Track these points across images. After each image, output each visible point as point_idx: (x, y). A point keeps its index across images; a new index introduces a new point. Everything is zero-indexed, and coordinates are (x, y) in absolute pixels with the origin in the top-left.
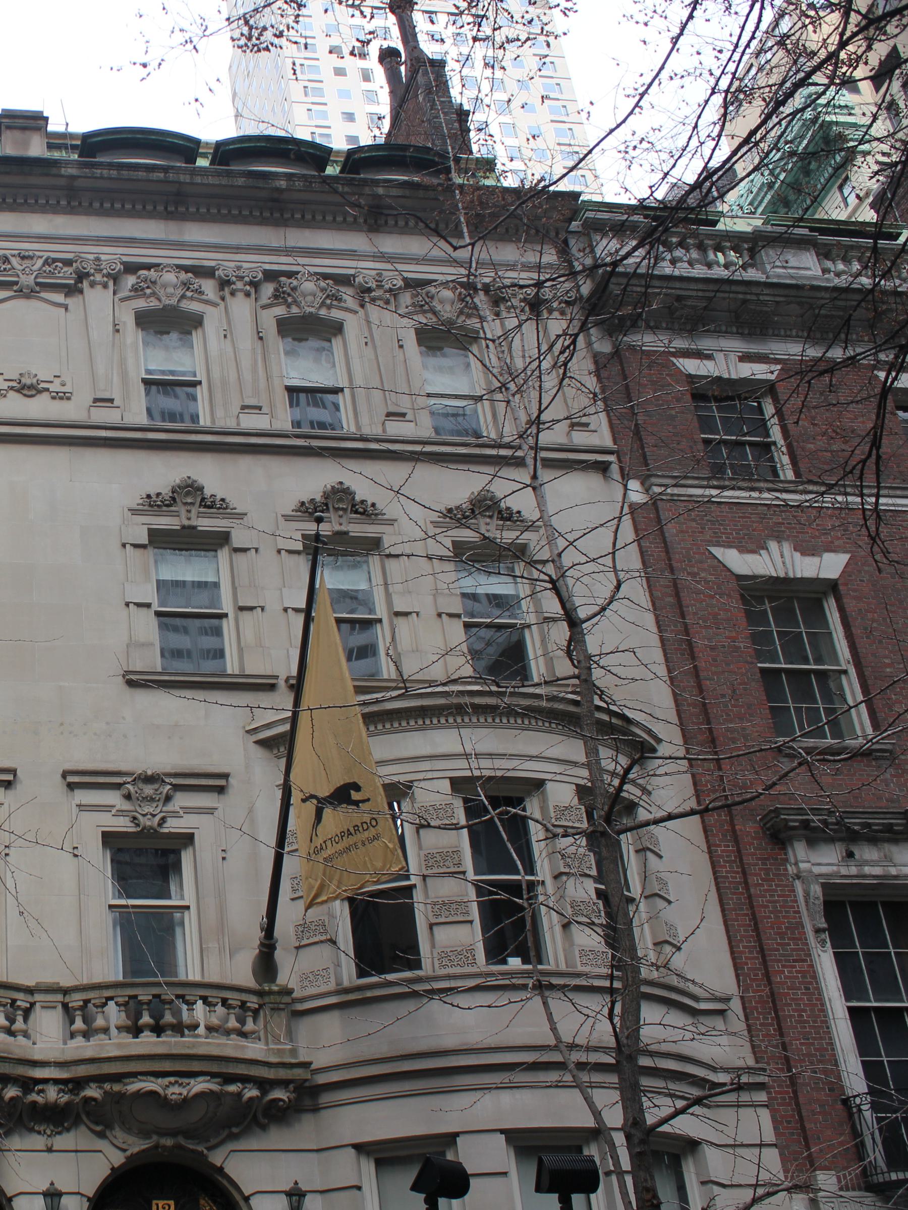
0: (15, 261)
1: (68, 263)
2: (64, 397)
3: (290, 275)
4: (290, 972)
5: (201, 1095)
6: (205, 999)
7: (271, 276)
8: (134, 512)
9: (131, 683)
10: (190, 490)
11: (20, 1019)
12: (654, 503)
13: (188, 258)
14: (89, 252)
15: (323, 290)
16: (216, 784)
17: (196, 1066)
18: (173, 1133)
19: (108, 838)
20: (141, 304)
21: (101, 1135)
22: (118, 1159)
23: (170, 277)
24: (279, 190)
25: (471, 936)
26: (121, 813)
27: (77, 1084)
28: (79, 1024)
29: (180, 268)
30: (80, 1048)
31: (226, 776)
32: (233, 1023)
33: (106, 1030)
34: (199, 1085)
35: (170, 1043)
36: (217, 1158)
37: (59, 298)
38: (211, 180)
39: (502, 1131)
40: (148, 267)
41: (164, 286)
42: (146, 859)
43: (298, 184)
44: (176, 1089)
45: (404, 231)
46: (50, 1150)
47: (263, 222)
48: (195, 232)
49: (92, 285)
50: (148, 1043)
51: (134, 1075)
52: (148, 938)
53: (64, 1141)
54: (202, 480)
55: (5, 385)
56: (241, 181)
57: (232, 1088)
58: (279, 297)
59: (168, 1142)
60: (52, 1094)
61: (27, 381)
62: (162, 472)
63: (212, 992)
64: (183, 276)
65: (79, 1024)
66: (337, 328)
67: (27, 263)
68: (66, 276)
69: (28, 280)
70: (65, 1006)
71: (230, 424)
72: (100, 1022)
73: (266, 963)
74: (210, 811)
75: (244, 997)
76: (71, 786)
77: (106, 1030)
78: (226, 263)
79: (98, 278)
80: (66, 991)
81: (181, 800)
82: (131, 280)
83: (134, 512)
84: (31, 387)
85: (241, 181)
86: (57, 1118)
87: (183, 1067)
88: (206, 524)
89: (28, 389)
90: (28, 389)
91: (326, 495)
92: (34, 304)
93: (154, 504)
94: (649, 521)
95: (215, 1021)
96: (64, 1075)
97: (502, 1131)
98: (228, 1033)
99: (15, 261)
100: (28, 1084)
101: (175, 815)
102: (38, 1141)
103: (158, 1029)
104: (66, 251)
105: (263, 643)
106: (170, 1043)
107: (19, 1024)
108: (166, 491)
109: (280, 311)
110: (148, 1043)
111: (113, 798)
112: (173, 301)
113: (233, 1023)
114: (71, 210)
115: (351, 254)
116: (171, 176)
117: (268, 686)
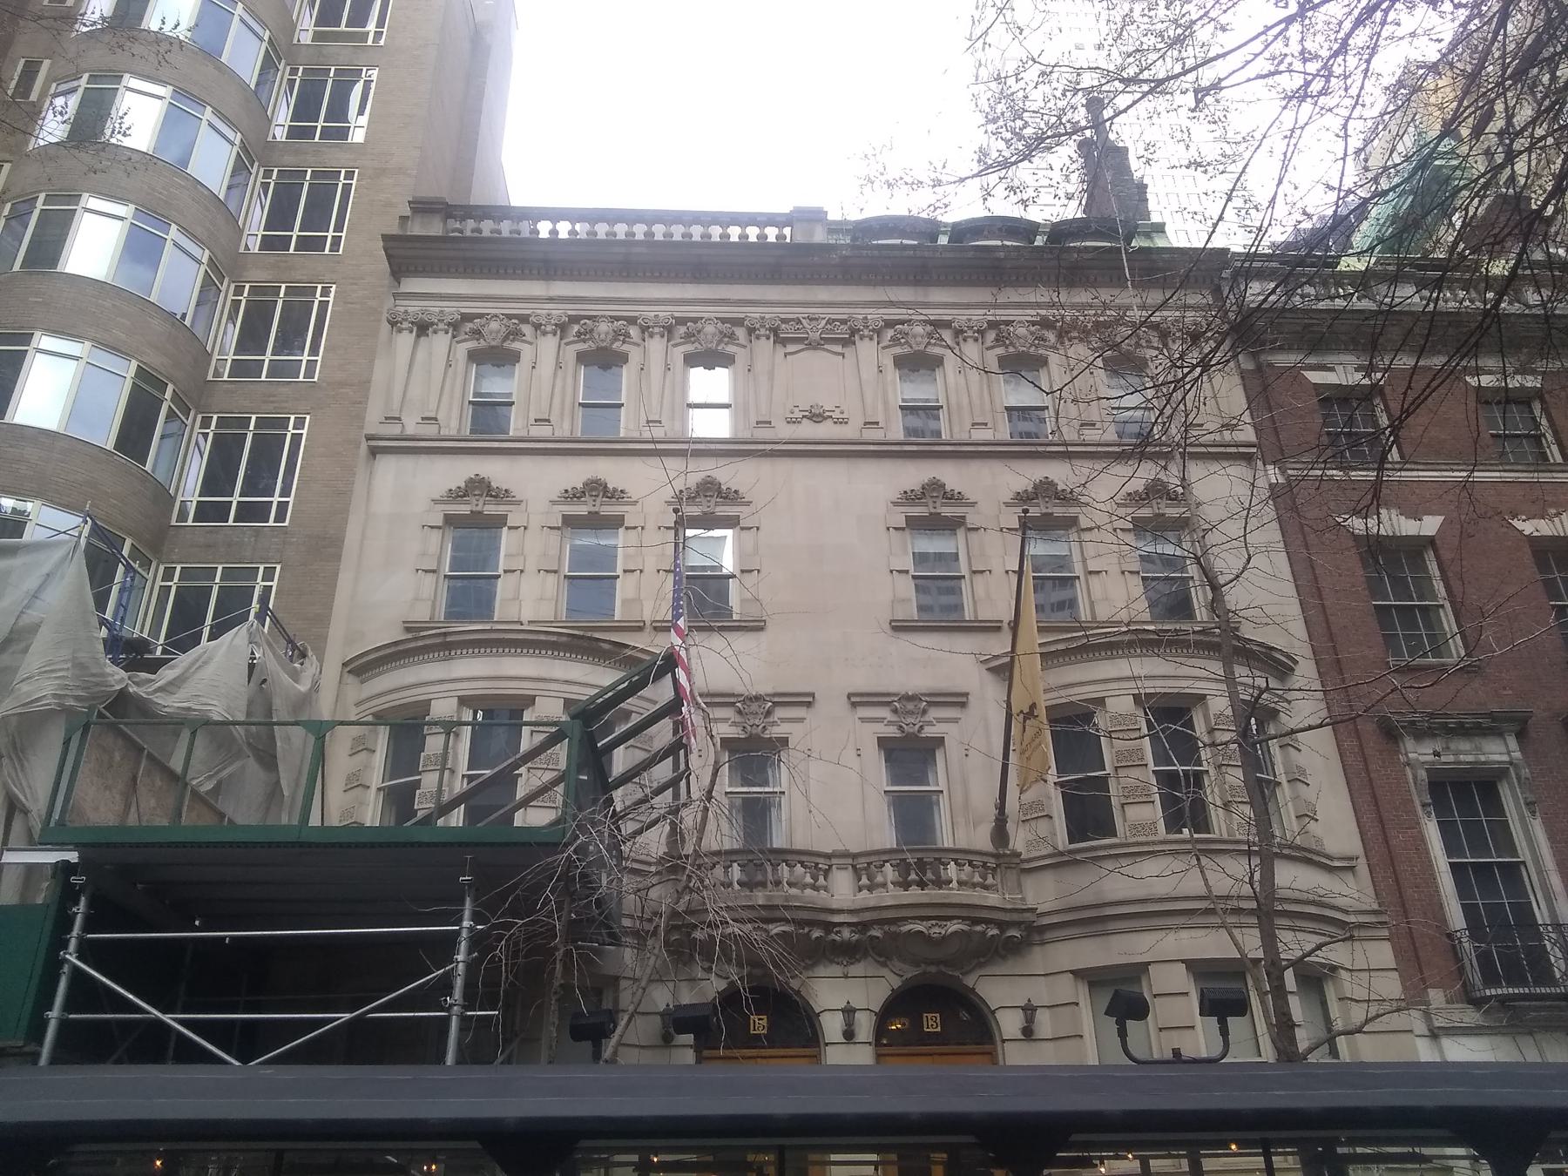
1: (844, 322)
2: (844, 422)
4: (1019, 840)
5: (956, 932)
6: (956, 861)
7: (993, 325)
8: (895, 504)
10: (934, 489)
11: (821, 879)
13: (933, 314)
14: (860, 313)
15: (1032, 333)
16: (959, 700)
17: (950, 912)
18: (938, 963)
19: (882, 742)
20: (898, 350)
21: (884, 965)
22: (897, 982)
23: (919, 329)
24: (999, 259)
25: (1153, 813)
26: (890, 723)
27: (863, 926)
28: (864, 881)
30: (867, 898)
31: (966, 695)
32: (977, 879)
33: (884, 885)
34: (954, 927)
35: (932, 894)
36: (969, 981)
37: (838, 348)
39: (1183, 961)
40: (902, 322)
41: (915, 336)
42: (909, 754)
44: (937, 930)
46: (846, 977)
50: (915, 894)
51: (905, 919)
52: (913, 814)
53: (857, 969)
54: (944, 479)
56: (970, 255)
57: (978, 928)
58: (999, 340)
59: (933, 969)
60: (846, 933)
62: (914, 475)
63: (962, 856)
64: (929, 328)
65: (864, 881)
70: (854, 867)
71: (964, 437)
72: (879, 879)
73: (1000, 833)
74: (956, 720)
75: (985, 859)
76: (854, 705)
77: (884, 885)
78: (961, 317)
79: (866, 332)
80: (855, 856)
81: (934, 713)
82: (890, 333)
83: (895, 504)
84: (819, 415)
86: (849, 953)
87: (942, 911)
88: (947, 511)
89: (816, 417)
90: (816, 417)
91: (1035, 487)
93: (909, 498)
95: (964, 877)
96: (854, 920)
97: (1183, 961)
98: (974, 885)
100: (829, 927)
101: (930, 723)
102: (836, 970)
103: (922, 884)
105: (991, 597)
106: (932, 894)
107: (821, 880)
108: (917, 488)
109: (1000, 351)
110: (915, 894)
111: (885, 713)
112: (922, 347)
113: (977, 879)
117: (999, 629)
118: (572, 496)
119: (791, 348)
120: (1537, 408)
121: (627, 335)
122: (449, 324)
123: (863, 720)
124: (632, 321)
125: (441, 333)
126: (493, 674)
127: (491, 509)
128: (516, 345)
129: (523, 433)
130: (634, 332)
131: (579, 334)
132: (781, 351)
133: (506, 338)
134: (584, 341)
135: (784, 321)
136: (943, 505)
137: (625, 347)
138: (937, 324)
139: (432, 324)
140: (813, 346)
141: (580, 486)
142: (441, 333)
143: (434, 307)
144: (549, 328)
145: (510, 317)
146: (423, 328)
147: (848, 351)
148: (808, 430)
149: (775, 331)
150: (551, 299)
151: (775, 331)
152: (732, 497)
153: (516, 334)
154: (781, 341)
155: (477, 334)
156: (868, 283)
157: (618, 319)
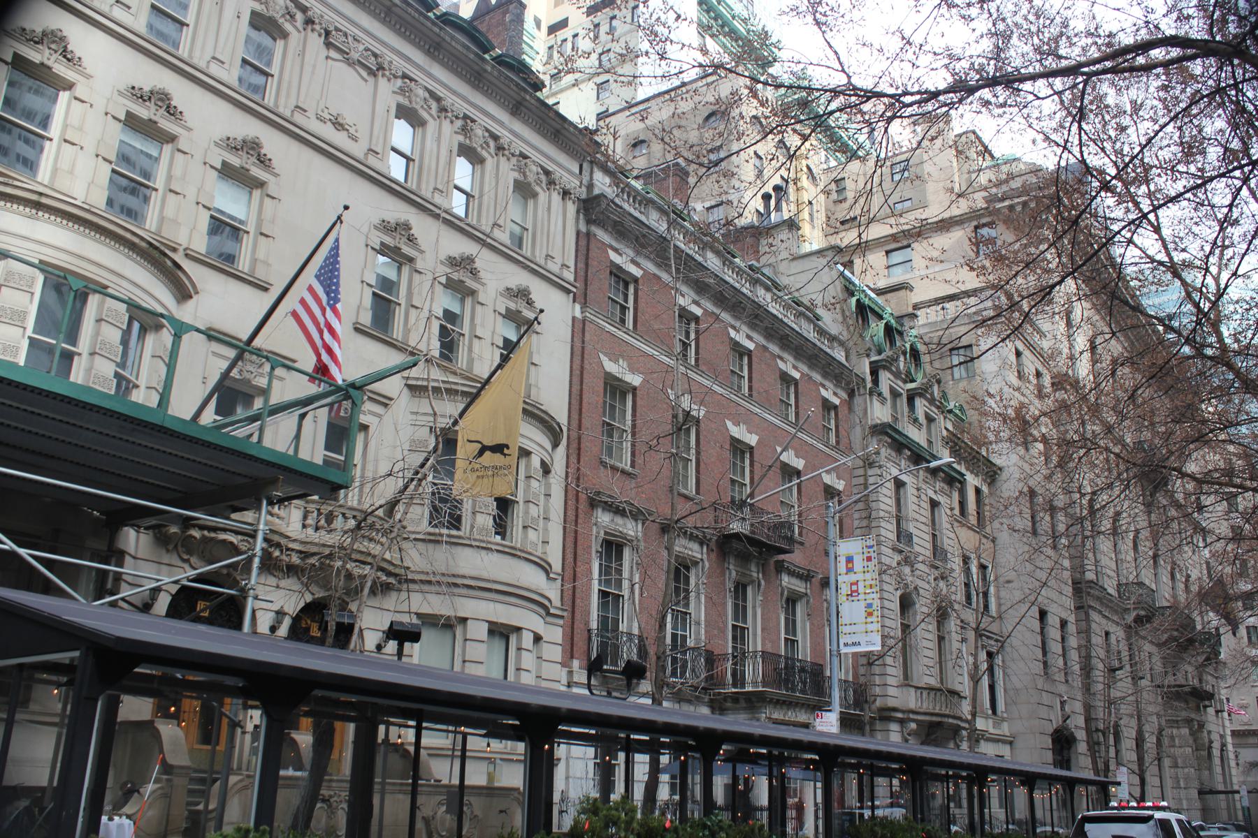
0: (350, 39)
1: (375, 55)
2: (355, 139)
3: (473, 121)
7: (466, 117)
9: (356, 329)
12: (584, 321)
14: (389, 56)
20: (401, 99)
23: (421, 92)
24: (486, 71)
29: (427, 89)
31: (391, 399)
37: (364, 74)
38: (459, 48)
40: (411, 80)
41: (417, 96)
43: (496, 73)
45: (525, 122)
47: (469, 82)
49: (383, 75)
55: (328, 117)
58: (402, 91)
62: (397, 211)
64: (427, 95)
66: (481, 161)
67: (356, 44)
74: (379, 416)
78: (449, 99)
82: (399, 82)
85: (472, 56)
88: (406, 250)
89: (338, 125)
90: (338, 125)
92: (351, 70)
93: (385, 227)
94: (579, 328)
99: (350, 39)
114: (384, 21)
115: (501, 124)
116: (442, 34)
119: (333, 54)
123: (214, 354)
132: (324, 52)
135: (337, 29)
136: (405, 243)
138: (432, 94)
140: (350, 63)
141: (147, 89)
147: (371, 80)
148: (328, 132)
149: (328, 33)
151: (328, 33)
154: (328, 45)
156: (399, 33)
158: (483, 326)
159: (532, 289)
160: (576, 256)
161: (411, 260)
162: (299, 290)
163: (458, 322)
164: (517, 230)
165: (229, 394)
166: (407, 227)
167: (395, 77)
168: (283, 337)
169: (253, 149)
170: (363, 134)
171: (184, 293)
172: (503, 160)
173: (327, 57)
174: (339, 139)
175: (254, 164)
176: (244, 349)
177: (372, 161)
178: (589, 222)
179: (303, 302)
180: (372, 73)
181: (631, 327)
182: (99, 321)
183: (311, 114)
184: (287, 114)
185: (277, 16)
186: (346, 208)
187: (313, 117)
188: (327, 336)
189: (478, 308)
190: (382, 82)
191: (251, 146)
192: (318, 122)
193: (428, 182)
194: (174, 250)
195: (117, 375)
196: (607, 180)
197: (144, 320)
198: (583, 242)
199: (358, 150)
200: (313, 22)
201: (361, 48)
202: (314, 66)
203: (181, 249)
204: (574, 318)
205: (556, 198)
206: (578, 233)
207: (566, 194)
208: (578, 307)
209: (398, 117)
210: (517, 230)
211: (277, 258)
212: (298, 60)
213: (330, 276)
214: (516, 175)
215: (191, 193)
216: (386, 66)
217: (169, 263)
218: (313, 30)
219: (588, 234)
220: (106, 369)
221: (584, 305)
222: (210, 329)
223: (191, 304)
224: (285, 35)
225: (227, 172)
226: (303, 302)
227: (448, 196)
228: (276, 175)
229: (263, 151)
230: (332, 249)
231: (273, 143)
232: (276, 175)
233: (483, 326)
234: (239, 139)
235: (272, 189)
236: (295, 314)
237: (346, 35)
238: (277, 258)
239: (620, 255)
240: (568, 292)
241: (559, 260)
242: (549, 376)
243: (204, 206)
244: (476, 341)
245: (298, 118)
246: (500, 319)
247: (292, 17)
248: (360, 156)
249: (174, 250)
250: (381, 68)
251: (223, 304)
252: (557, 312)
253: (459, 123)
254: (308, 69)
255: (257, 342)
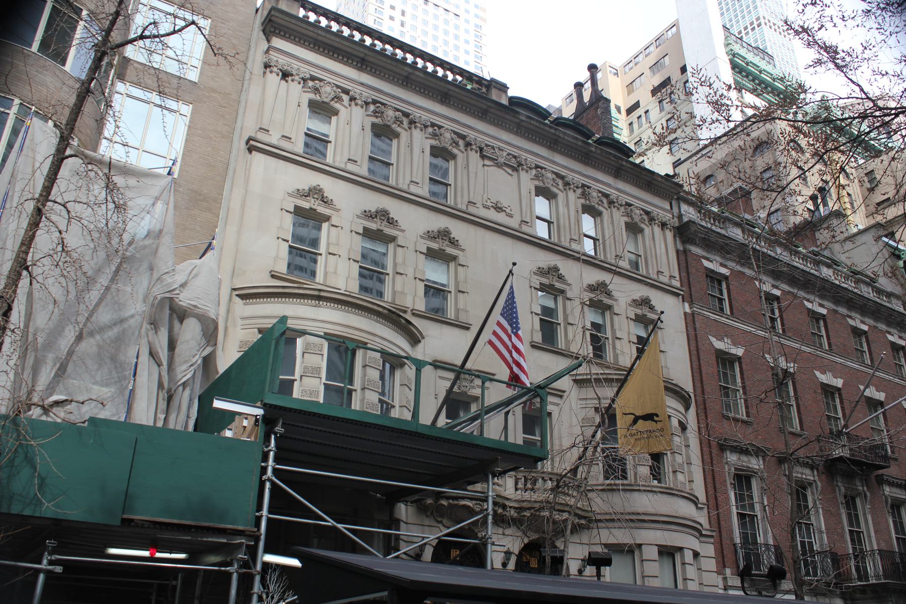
0: (496, 150)
1: (515, 157)
2: (511, 216)
3: (589, 187)
7: (583, 186)
9: (533, 346)
12: (693, 314)
14: (524, 155)
23: (550, 175)
24: (591, 151)
27: (520, 510)
29: (553, 172)
31: (564, 392)
37: (510, 171)
40: (542, 168)
41: (547, 178)
43: (598, 151)
45: (626, 181)
48: (559, 158)
55: (491, 205)
56: (580, 143)
58: (537, 177)
61: (499, 205)
62: (547, 259)
64: (554, 176)
67: (501, 153)
68: (513, 163)
69: (502, 160)
74: (558, 405)
78: (570, 176)
79: (474, 147)
82: (534, 172)
85: (580, 143)
88: (558, 285)
89: (498, 208)
90: (498, 208)
93: (541, 272)
94: (690, 320)
99: (496, 150)
104: (516, 152)
105: (575, 339)
115: (609, 185)
118: (369, 215)
119: (487, 162)
120: (776, 304)
121: (402, 122)
122: (303, 79)
123: (441, 378)
124: (406, 115)
125: (274, 74)
126: (346, 323)
127: (322, 209)
128: (337, 106)
129: (342, 166)
130: (406, 121)
131: (375, 112)
132: (481, 162)
133: (333, 99)
134: (377, 117)
135: (487, 145)
136: (557, 281)
137: (399, 129)
138: (558, 175)
139: (292, 75)
140: (499, 166)
142: (274, 74)
143: (296, 64)
144: (359, 102)
145: (338, 87)
146: (285, 75)
147: (515, 174)
148: (492, 215)
149: (481, 149)
150: (362, 84)
151: (481, 149)
152: (454, 243)
153: (338, 99)
154: (483, 157)
155: (316, 90)
157: (398, 110)
158: (620, 330)
159: (651, 298)
160: (679, 269)
161: (563, 292)
162: (491, 326)
163: (603, 329)
164: (633, 257)
165: (454, 403)
166: (556, 269)
167: (531, 169)
168: (486, 359)
169: (445, 236)
170: (515, 211)
171: (415, 339)
172: (614, 210)
173: (484, 165)
174: (500, 218)
175: (447, 246)
176: (460, 372)
177: (525, 228)
178: (683, 242)
179: (495, 333)
180: (515, 169)
181: (729, 313)
182: (365, 366)
183: (479, 205)
184: (464, 208)
185: (447, 146)
186: (514, 264)
187: (481, 207)
188: (515, 354)
189: (615, 317)
190: (523, 174)
191: (444, 234)
192: (485, 210)
193: (565, 236)
194: (405, 312)
195: (380, 401)
196: (691, 210)
197: (394, 362)
198: (682, 258)
199: (514, 223)
200: (471, 145)
201: (505, 154)
202: (476, 173)
203: (409, 310)
204: (685, 313)
205: (657, 230)
206: (677, 252)
207: (663, 225)
208: (687, 305)
209: (537, 195)
210: (633, 257)
211: (473, 305)
212: (465, 172)
213: (510, 312)
214: (626, 219)
215: (410, 272)
216: (523, 162)
217: (403, 321)
218: (471, 150)
219: (685, 251)
220: (373, 397)
221: (691, 304)
222: (435, 361)
223: (420, 346)
224: (454, 157)
225: (431, 254)
226: (495, 333)
227: (580, 242)
228: (463, 250)
229: (452, 236)
230: (509, 294)
231: (458, 230)
232: (463, 250)
233: (620, 330)
234: (436, 231)
235: (462, 260)
236: (490, 343)
237: (493, 148)
238: (473, 305)
239: (711, 261)
240: (677, 295)
241: (667, 274)
242: (675, 358)
243: (420, 280)
244: (617, 342)
245: (472, 209)
246: (632, 323)
247: (457, 144)
248: (516, 226)
249: (405, 312)
250: (520, 164)
251: (442, 343)
252: (672, 311)
253: (579, 191)
254: (472, 175)
255: (468, 365)
